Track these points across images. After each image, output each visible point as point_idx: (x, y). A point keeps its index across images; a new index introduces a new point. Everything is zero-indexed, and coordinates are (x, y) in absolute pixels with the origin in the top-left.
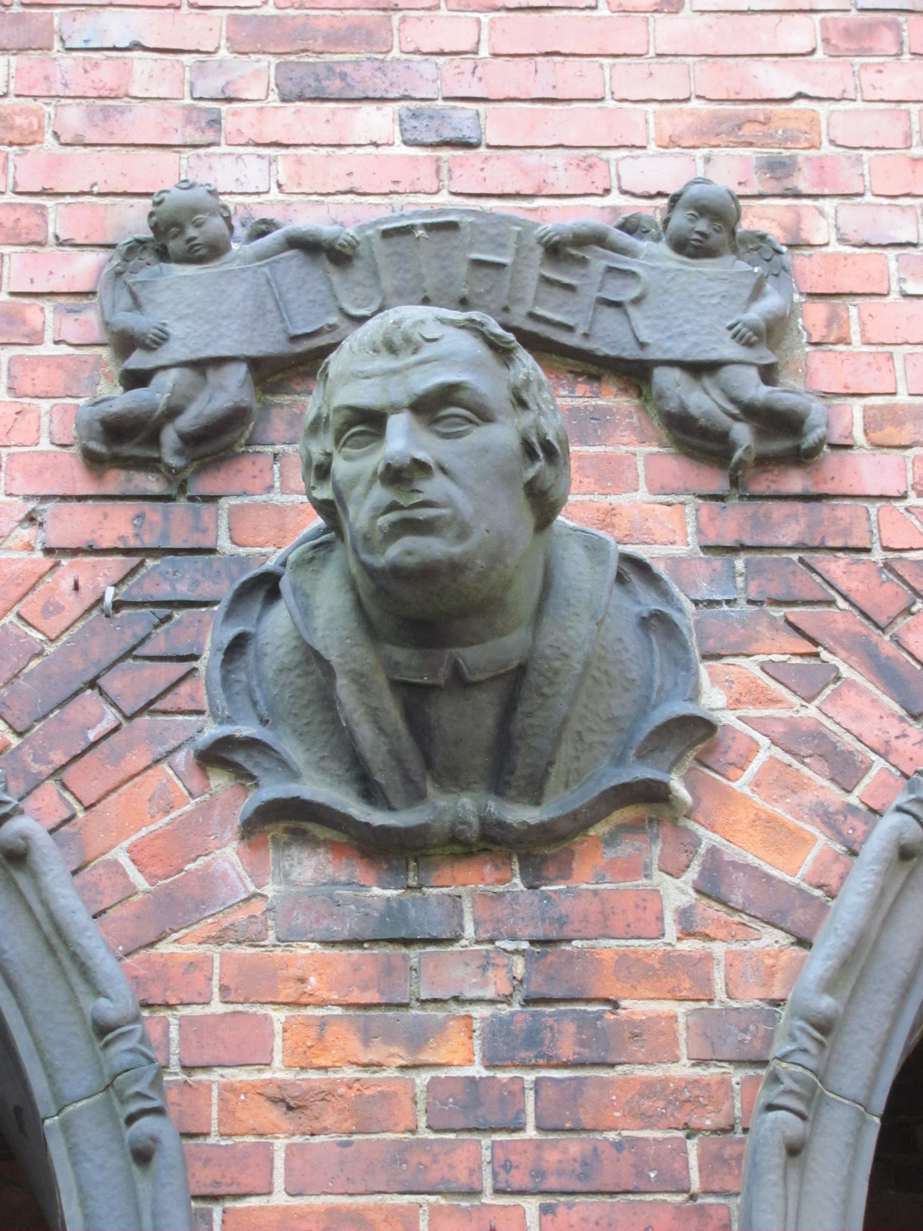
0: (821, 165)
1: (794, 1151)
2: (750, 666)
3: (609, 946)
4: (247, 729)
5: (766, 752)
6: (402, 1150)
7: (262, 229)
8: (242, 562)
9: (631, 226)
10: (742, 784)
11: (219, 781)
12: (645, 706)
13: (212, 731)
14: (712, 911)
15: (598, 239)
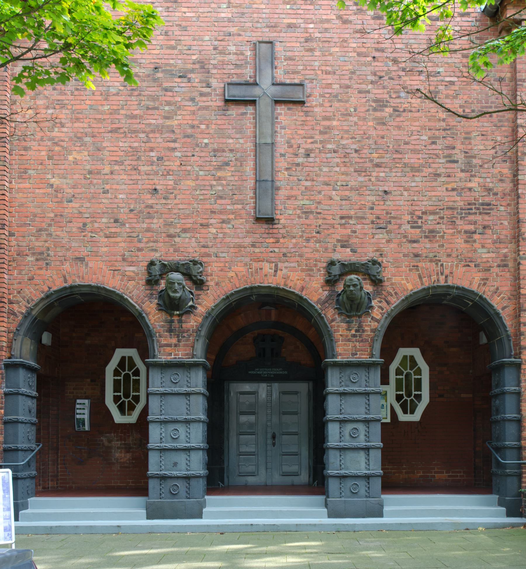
0: (385, 255)
1: (377, 340)
2: (376, 301)
3: (364, 324)
4: (338, 306)
5: (377, 308)
6: (349, 339)
7: (339, 262)
8: (338, 292)
9: (369, 261)
10: (375, 311)
11: (336, 310)
12: (368, 305)
13: (335, 307)
14: (372, 321)
15: (366, 263)
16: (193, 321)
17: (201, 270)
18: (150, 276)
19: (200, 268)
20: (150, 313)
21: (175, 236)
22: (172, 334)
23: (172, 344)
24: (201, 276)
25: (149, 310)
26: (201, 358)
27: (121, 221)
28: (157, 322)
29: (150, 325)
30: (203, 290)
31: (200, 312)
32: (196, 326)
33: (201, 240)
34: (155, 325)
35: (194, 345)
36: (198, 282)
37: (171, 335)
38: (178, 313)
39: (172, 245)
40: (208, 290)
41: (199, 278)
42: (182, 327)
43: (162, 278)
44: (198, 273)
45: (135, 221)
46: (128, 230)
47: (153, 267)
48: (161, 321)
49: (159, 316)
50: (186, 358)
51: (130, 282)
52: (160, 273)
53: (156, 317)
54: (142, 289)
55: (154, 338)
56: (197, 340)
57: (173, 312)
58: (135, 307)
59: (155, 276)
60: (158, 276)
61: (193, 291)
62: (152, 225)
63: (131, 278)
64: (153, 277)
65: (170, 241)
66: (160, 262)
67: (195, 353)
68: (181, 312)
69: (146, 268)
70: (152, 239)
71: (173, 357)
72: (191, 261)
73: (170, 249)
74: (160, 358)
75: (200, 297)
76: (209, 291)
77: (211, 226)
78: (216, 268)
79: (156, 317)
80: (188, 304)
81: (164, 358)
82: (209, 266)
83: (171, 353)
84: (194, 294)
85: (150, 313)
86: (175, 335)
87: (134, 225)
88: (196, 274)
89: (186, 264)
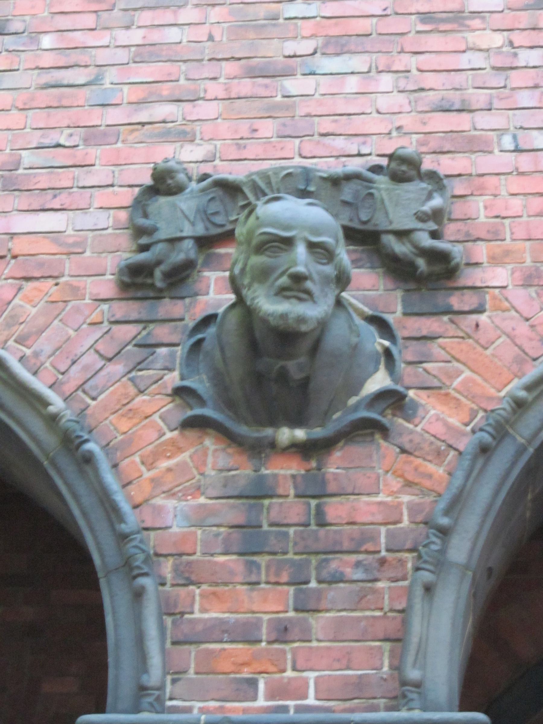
16: (396, 484)
17: (437, 201)
18: (144, 248)
19: (430, 197)
20: (128, 442)
21: (289, 73)
22: (263, 560)
23: (257, 625)
24: (435, 235)
25: (124, 425)
26: (451, 710)
27: (16, 26)
28: (170, 494)
29: (125, 507)
30: (449, 311)
31: (438, 429)
32: (413, 509)
33: (430, 80)
34: (159, 510)
35: (405, 623)
36: (421, 263)
37: (251, 566)
38: (300, 434)
39: (277, 107)
40: (480, 310)
41: (426, 241)
42: (322, 524)
43: (208, 263)
44: (422, 217)
45: (89, 20)
46: (48, 60)
47: (163, 200)
48: (198, 490)
49: (185, 456)
50: (345, 711)
51: (28, 286)
52: (200, 230)
53: (165, 464)
54: (94, 317)
55: (146, 582)
56: (428, 589)
57: (269, 431)
58: (46, 403)
59: (173, 241)
60: (189, 244)
61: (390, 318)
62: (175, 29)
63: (41, 265)
64: (158, 249)
65: (262, 92)
66: (204, 177)
67: (414, 674)
68: (318, 432)
69: (123, 215)
70: (166, 90)
71: (261, 702)
72: (376, 169)
73: (258, 124)
74: (174, 710)
75: (435, 348)
76: (483, 318)
77: (476, 23)
78: (517, 204)
79: (165, 464)
80: (361, 385)
81: (202, 710)
82: (481, 191)
83: (253, 683)
84: (400, 334)
85: (128, 442)
86: (280, 566)
87: (79, 38)
88: (410, 224)
89: (349, 177)
